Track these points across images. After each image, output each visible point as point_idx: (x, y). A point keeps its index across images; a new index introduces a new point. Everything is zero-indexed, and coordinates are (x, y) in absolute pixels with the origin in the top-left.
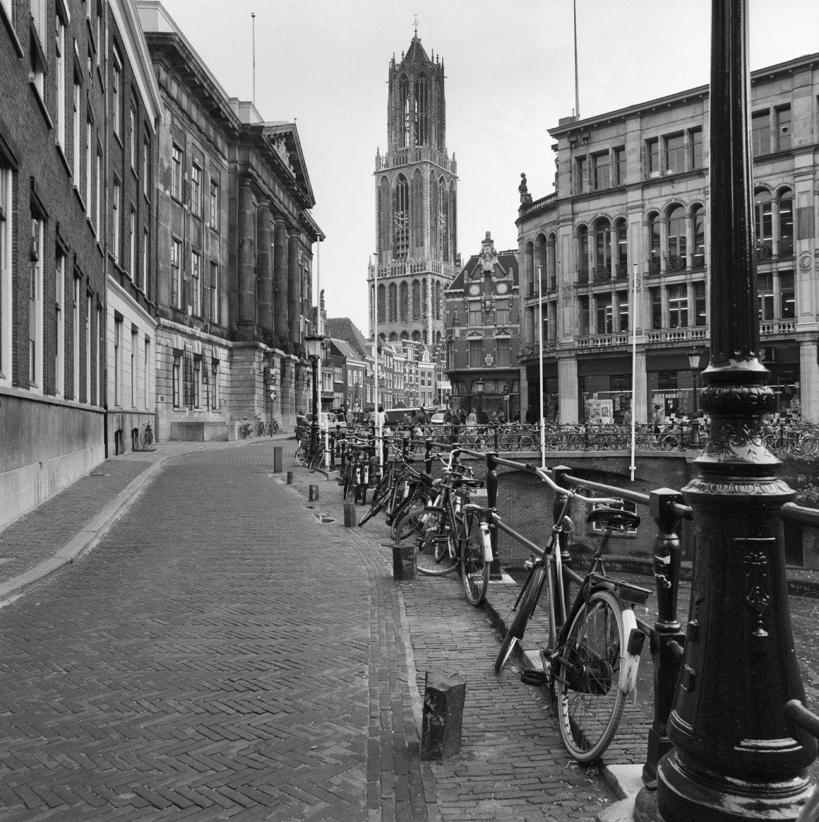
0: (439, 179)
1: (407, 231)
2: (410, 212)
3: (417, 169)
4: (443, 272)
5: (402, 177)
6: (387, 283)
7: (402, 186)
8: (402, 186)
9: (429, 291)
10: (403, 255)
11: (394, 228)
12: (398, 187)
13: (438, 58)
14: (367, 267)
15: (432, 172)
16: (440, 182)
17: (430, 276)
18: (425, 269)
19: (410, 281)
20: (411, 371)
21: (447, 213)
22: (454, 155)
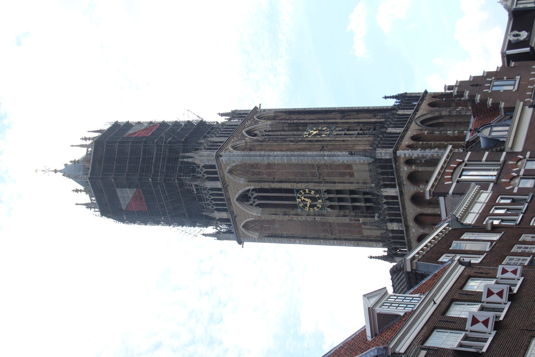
0: (248, 138)
1: (328, 192)
2: (295, 186)
3: (230, 172)
5: (244, 198)
7: (257, 198)
8: (257, 198)
10: (367, 200)
11: (323, 215)
12: (257, 205)
13: (86, 139)
15: (235, 148)
16: (255, 135)
17: (400, 153)
18: (389, 161)
19: (410, 189)
21: (305, 125)
22: (222, 115)
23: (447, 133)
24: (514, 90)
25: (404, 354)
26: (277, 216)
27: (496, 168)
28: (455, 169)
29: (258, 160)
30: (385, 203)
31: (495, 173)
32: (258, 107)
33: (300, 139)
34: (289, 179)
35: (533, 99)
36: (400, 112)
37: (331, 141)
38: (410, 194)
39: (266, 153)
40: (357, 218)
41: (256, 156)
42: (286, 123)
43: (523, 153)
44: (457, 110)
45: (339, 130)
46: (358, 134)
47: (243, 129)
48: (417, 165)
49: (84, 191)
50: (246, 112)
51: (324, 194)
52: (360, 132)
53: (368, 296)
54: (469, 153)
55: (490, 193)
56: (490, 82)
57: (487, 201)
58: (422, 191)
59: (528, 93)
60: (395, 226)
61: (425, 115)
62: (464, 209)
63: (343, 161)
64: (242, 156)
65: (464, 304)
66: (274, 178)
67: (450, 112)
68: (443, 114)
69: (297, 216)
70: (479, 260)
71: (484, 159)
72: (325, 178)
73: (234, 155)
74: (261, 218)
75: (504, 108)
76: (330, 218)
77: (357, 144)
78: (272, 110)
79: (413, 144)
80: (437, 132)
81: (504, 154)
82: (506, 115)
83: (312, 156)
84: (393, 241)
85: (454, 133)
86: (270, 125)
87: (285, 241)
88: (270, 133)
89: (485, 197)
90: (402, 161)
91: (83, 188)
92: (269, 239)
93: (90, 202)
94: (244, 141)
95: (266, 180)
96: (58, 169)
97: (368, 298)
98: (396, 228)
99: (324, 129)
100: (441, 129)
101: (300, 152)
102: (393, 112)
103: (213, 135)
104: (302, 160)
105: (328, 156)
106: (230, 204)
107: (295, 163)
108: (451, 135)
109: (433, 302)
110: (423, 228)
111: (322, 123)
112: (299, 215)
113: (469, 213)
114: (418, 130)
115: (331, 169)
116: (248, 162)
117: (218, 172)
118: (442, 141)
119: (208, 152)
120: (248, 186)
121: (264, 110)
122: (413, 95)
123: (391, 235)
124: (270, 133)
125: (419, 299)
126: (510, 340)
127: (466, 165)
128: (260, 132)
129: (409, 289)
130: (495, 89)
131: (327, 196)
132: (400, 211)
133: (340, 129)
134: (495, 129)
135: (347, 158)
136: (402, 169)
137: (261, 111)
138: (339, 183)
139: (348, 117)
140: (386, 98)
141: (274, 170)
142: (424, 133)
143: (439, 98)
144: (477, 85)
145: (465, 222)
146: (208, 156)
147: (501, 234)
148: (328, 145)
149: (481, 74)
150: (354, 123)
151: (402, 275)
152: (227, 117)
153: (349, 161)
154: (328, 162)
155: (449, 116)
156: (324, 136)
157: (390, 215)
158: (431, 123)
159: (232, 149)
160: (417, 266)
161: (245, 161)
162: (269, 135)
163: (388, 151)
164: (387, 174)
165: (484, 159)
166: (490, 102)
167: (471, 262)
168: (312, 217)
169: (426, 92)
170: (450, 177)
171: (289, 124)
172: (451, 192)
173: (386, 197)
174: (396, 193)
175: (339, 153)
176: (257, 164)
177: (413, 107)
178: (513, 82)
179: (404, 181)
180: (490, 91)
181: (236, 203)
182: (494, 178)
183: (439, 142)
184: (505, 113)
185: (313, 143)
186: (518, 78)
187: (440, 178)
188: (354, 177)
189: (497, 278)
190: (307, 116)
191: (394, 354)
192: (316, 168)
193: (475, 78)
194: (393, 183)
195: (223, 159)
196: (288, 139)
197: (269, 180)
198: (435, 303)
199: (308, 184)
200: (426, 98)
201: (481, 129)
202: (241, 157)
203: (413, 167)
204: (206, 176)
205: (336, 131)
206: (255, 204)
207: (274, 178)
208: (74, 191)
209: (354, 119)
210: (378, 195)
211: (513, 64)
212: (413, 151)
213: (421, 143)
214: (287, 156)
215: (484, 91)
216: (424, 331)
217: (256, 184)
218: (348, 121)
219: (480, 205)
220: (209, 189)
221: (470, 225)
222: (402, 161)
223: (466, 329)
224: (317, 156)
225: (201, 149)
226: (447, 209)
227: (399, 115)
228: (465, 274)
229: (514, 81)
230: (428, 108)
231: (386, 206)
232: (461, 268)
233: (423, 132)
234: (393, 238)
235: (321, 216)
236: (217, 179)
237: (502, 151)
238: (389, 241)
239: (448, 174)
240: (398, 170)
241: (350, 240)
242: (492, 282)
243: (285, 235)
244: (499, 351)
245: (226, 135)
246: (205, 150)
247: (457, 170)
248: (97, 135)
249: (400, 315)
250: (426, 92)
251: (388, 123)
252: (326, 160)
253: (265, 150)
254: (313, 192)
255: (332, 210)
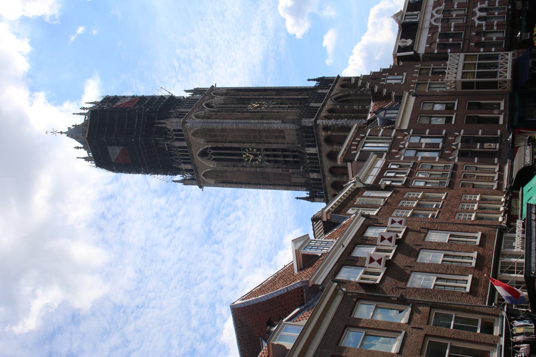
0: (207, 109)
1: (266, 150)
3: (193, 134)
4: (317, 105)
5: (204, 154)
6: (329, 179)
9: (340, 122)
10: (295, 156)
11: (263, 167)
13: (84, 109)
14: (309, 202)
15: (197, 117)
16: (212, 107)
17: (319, 122)
18: (311, 127)
19: (326, 149)
20: (412, 147)
21: (250, 100)
22: (187, 91)
23: (353, 107)
24: (402, 83)
25: (321, 285)
26: (228, 167)
27: (388, 141)
28: (359, 142)
29: (214, 126)
30: (308, 159)
31: (388, 145)
32: (214, 85)
33: (246, 110)
34: (237, 140)
35: (416, 90)
36: (320, 91)
37: (268, 112)
38: (326, 152)
39: (220, 121)
40: (287, 170)
41: (212, 123)
42: (235, 98)
43: (408, 130)
44: (361, 90)
45: (275, 104)
46: (289, 107)
47: (203, 103)
48: (332, 131)
49: (83, 148)
50: (205, 90)
51: (263, 152)
52: (291, 106)
53: (295, 241)
54: (369, 130)
55: (384, 160)
56: (385, 77)
57: (381, 167)
58: (335, 150)
59: (411, 86)
60: (315, 176)
61: (337, 93)
62: (365, 173)
63: (277, 128)
64: (202, 123)
65: (365, 247)
66: (226, 140)
67: (356, 92)
68: (350, 93)
69: (243, 168)
70: (375, 213)
71: (380, 134)
72: (264, 140)
73: (196, 122)
74: (216, 169)
75: (395, 96)
76: (268, 169)
77: (288, 115)
78: (225, 88)
79: (328, 115)
80: (347, 106)
81: (394, 131)
82: (396, 101)
83: (254, 123)
84: (313, 186)
85: (358, 107)
86: (223, 100)
87: (234, 186)
88: (223, 106)
89: (380, 163)
90: (320, 128)
91: (82, 146)
92: (222, 184)
93: (88, 156)
94: (203, 112)
95: (220, 141)
96: (63, 131)
97: (296, 243)
98: (315, 177)
99: (263, 103)
100: (349, 104)
101: (245, 120)
102: (314, 91)
103: (180, 107)
104: (247, 126)
105: (266, 123)
106: (194, 158)
107: (242, 128)
108: (357, 109)
109: (342, 245)
110: (336, 177)
111: (262, 99)
112: (245, 167)
113: (369, 176)
114: (332, 105)
115: (269, 133)
116: (207, 127)
117: (184, 135)
118: (350, 113)
119: (176, 120)
120: (206, 145)
121: (219, 88)
122: (329, 78)
123: (312, 182)
124: (223, 106)
125: (332, 243)
126: (396, 274)
127: (367, 139)
128: (216, 105)
129: (326, 232)
130: (388, 82)
131: (265, 153)
132: (319, 164)
133: (276, 103)
134: (388, 112)
135: (280, 125)
136: (320, 134)
137: (216, 89)
138: (274, 143)
139: (281, 94)
140: (309, 80)
141: (226, 134)
142: (337, 107)
143: (348, 81)
144: (375, 79)
145: (366, 183)
146: (177, 122)
147: (392, 192)
148: (266, 115)
149: (379, 71)
150: (286, 99)
151: (320, 223)
152: (191, 93)
153: (282, 127)
154: (266, 128)
155: (356, 95)
156: (263, 108)
157: (311, 167)
158: (342, 99)
159: (194, 118)
160: (331, 217)
161: (204, 127)
162: (222, 107)
163: (311, 121)
164: (309, 137)
165: (380, 134)
166: (385, 92)
167: (370, 214)
168: (254, 168)
169: (339, 76)
170: (356, 147)
171: (238, 99)
172: (356, 159)
173: (309, 154)
174: (316, 151)
175: (275, 121)
176: (213, 129)
177: (329, 88)
178: (401, 77)
179: (322, 143)
180: (385, 84)
181: (198, 157)
182: (387, 149)
183: (348, 114)
184: (395, 100)
185: (255, 114)
186: (405, 74)
187: (348, 149)
188: (285, 139)
189: (388, 227)
190: (251, 93)
191: (313, 285)
192: (258, 132)
193: (375, 73)
194: (314, 144)
195: (188, 125)
196: (237, 110)
197: (223, 141)
198: (343, 246)
199: (251, 144)
200: (339, 81)
201: (378, 112)
202: (201, 124)
203: (329, 133)
204: (175, 137)
205: (273, 104)
206: (212, 158)
207: (226, 140)
208: (75, 148)
209: (286, 96)
210: (303, 153)
211: (401, 63)
212: (329, 120)
213: (335, 114)
214: (236, 123)
215: (381, 83)
216: (335, 268)
217: (213, 143)
218: (281, 97)
219: (377, 169)
220: (178, 148)
221: (369, 185)
222: (320, 128)
223: (365, 266)
224: (258, 123)
225: (171, 117)
226: (353, 172)
227: (319, 93)
228: (366, 223)
229: (402, 77)
230: (340, 88)
231: (308, 161)
232: (363, 219)
233: (336, 107)
234: (314, 184)
235: (260, 168)
236: (183, 140)
237: (393, 128)
238: (311, 186)
239: (354, 145)
240: (318, 135)
241: (282, 185)
242: (385, 230)
243: (234, 182)
244: (388, 283)
245: (190, 107)
246: (174, 118)
247: (361, 143)
248: (92, 105)
249: (318, 255)
250: (339, 76)
251: (311, 99)
252: (265, 127)
253: (219, 119)
254: (255, 150)
255: (269, 164)
